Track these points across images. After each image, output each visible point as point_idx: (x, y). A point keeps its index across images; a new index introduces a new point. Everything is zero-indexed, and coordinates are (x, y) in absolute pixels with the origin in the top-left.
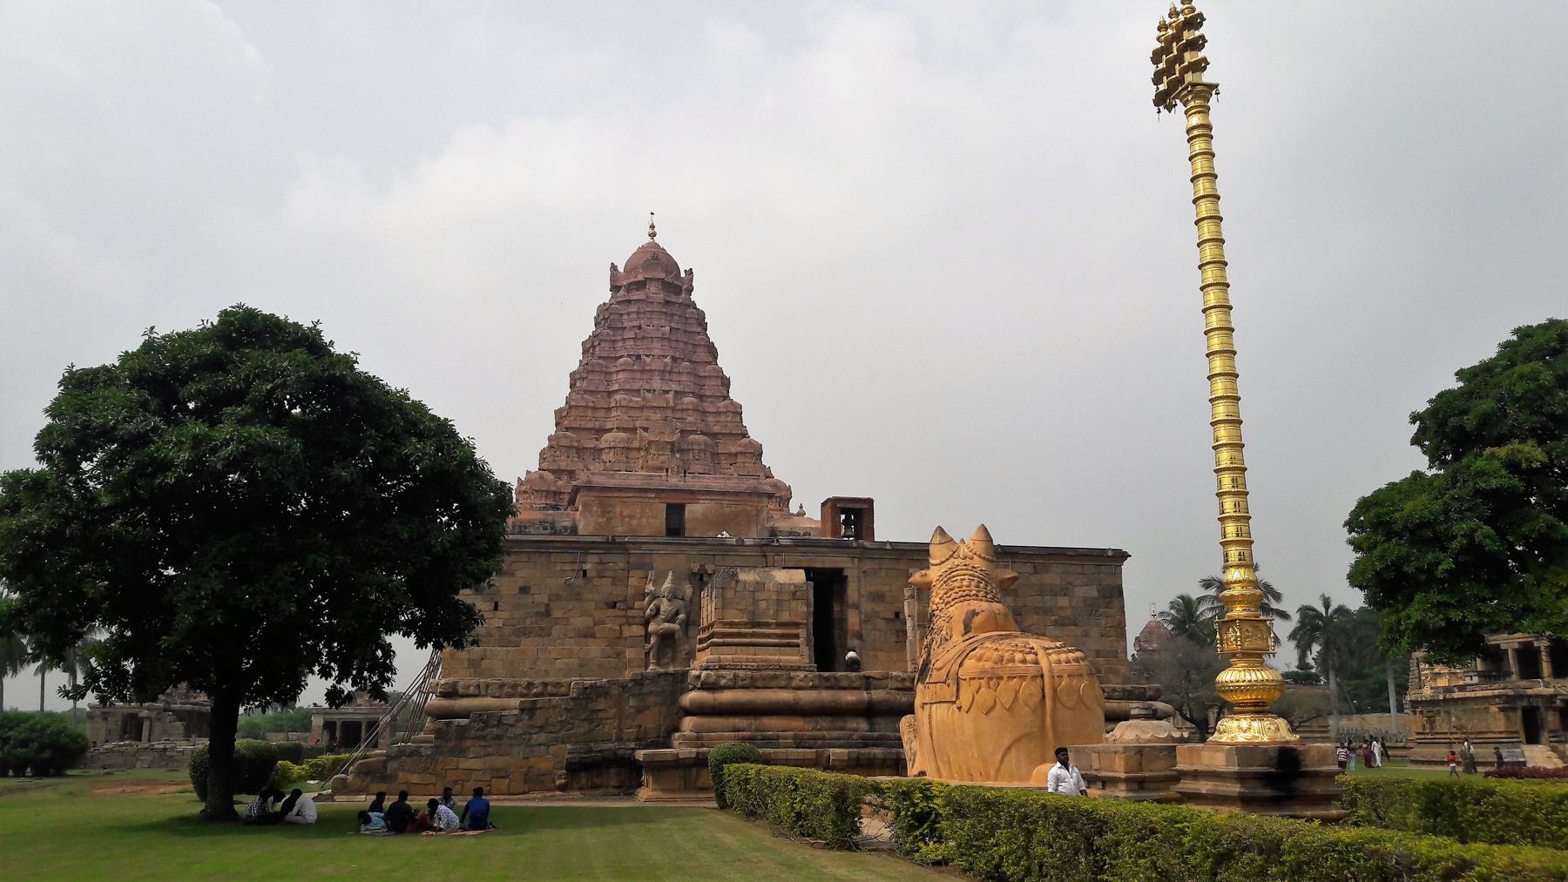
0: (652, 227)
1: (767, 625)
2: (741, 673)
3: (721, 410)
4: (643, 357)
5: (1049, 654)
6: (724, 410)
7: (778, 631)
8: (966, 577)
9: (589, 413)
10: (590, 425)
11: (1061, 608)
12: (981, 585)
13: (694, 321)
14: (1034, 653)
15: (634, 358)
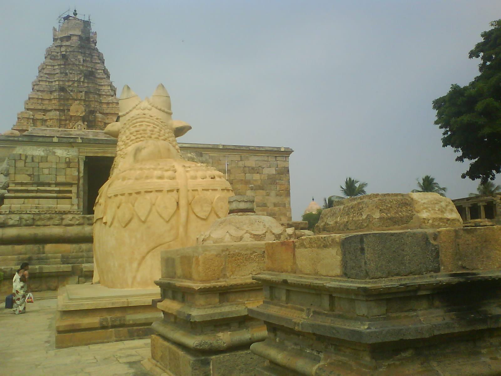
0: (75, 11)
1: (49, 185)
2: (25, 216)
3: (110, 102)
4: (68, 74)
5: (187, 171)
6: (112, 102)
7: (57, 189)
8: (144, 123)
9: (40, 101)
10: (40, 107)
11: (256, 180)
12: (156, 130)
13: (97, 57)
14: (173, 170)
15: (64, 74)
